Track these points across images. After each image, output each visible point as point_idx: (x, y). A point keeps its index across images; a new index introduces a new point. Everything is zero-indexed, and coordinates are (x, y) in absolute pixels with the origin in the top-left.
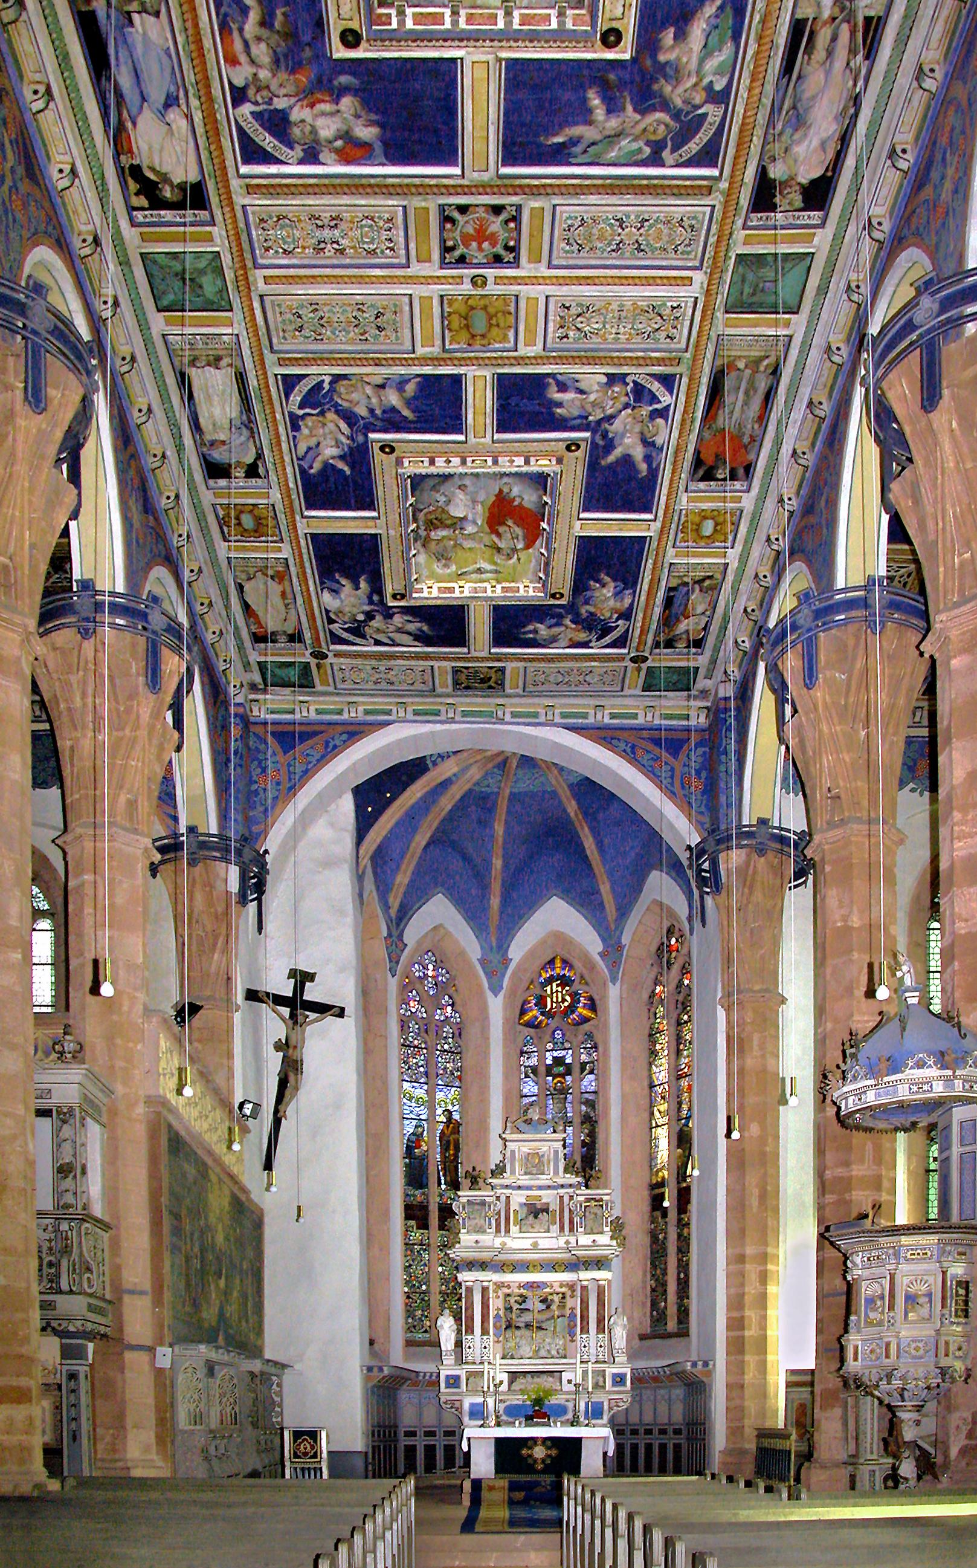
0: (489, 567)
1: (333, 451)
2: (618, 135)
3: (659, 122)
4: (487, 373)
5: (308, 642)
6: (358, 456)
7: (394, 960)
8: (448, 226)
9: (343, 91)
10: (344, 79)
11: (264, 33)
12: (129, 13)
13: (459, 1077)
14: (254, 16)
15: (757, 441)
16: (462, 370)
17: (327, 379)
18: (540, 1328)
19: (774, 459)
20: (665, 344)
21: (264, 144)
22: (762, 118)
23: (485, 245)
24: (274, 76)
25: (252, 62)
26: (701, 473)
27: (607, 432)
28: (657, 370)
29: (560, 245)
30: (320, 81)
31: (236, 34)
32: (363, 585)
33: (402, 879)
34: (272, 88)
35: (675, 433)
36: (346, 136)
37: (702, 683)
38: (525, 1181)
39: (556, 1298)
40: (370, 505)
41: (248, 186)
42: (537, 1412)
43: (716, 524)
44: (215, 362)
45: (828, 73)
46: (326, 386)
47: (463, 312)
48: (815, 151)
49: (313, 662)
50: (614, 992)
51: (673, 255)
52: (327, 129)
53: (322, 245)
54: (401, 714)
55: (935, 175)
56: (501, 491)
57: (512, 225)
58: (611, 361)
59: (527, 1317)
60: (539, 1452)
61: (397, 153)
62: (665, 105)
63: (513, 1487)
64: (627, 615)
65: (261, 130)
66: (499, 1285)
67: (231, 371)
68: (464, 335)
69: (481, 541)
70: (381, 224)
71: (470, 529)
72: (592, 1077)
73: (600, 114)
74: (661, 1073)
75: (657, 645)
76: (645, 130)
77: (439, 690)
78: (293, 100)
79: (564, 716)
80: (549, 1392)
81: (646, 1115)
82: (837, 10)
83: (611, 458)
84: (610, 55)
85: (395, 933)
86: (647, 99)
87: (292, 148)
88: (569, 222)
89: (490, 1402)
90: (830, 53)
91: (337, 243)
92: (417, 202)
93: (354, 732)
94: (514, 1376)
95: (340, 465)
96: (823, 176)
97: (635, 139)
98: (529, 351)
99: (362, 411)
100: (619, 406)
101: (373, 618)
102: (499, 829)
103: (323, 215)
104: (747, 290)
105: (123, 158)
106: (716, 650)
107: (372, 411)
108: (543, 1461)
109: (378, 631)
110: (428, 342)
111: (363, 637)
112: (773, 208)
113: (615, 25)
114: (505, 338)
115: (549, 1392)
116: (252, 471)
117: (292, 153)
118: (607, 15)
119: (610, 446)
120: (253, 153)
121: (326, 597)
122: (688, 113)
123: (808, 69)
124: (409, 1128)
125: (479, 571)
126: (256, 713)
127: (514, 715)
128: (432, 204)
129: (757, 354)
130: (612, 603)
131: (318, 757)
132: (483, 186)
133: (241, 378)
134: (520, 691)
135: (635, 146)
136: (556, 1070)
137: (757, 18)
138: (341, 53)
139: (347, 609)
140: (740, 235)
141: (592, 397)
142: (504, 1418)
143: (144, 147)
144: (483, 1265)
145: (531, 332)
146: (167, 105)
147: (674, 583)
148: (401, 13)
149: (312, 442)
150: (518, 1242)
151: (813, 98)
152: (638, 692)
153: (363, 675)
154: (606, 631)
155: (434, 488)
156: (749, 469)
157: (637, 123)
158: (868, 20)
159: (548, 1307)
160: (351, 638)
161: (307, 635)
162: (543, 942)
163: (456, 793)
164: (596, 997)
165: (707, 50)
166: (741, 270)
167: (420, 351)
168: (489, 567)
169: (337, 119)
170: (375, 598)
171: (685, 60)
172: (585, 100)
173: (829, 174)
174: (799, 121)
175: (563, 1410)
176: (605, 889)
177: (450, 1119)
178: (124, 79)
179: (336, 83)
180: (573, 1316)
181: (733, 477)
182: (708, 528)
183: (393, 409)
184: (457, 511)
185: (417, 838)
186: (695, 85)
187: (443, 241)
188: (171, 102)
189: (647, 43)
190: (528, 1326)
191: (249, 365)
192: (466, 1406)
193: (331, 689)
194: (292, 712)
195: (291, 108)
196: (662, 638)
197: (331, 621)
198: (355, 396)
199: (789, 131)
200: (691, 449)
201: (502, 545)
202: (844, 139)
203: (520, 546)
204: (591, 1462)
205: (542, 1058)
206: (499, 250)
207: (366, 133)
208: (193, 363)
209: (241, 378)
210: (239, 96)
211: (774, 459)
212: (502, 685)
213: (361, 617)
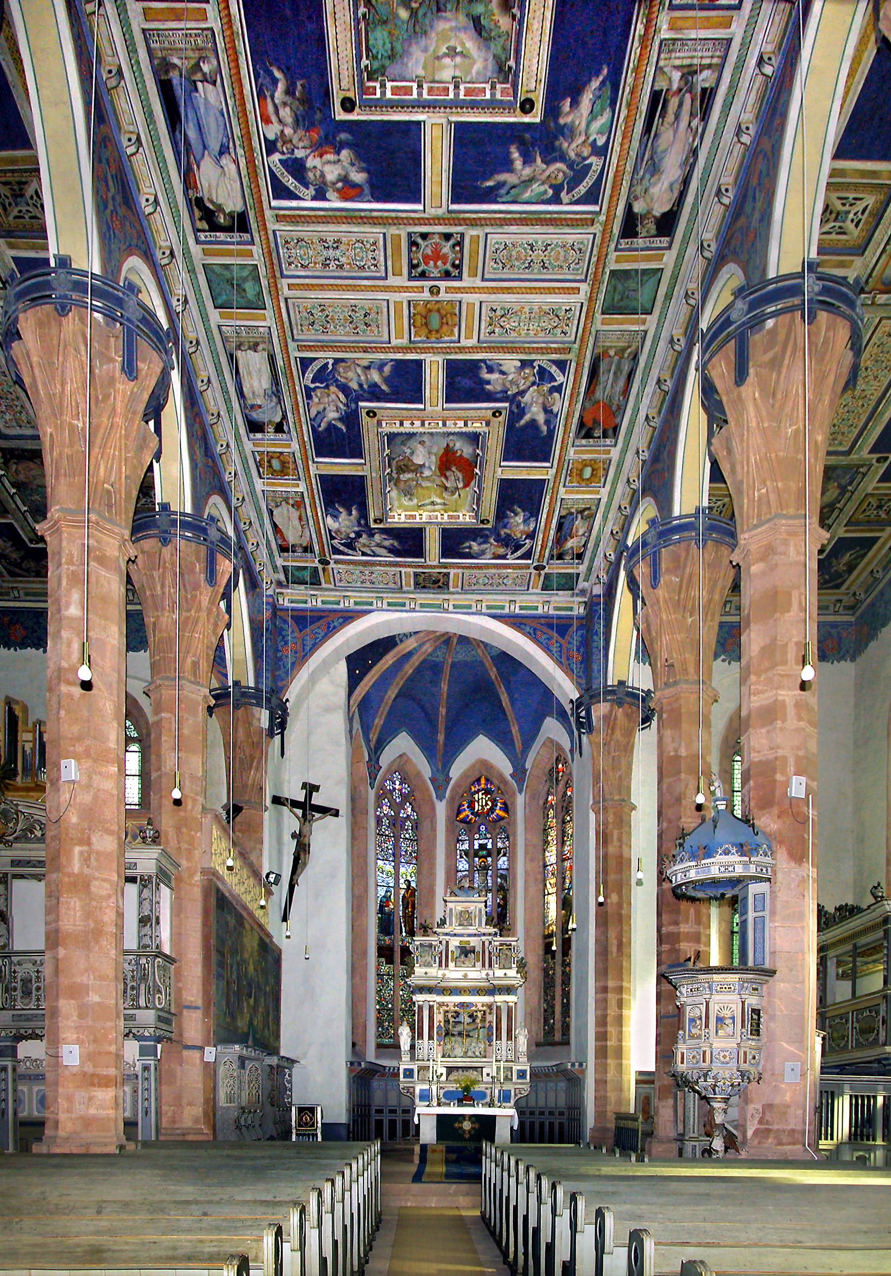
0: (439, 501)
1: (336, 415)
2: (531, 180)
3: (559, 170)
4: (440, 358)
5: (317, 552)
6: (351, 418)
7: (373, 776)
10: (343, 136)
11: (289, 99)
13: (416, 858)
14: (281, 86)
15: (622, 409)
16: (422, 356)
17: (331, 362)
18: (468, 1036)
19: (632, 423)
20: (560, 337)
21: (288, 184)
22: (629, 168)
23: (439, 263)
25: (280, 121)
26: (583, 432)
27: (520, 402)
28: (554, 357)
29: (490, 264)
30: (326, 136)
32: (354, 512)
33: (379, 722)
34: (294, 142)
35: (566, 404)
36: (345, 179)
37: (582, 584)
38: (459, 930)
39: (479, 1014)
40: (360, 456)
42: (466, 1096)
43: (593, 470)
44: (254, 347)
45: (675, 132)
46: (330, 367)
47: (424, 313)
48: (666, 191)
49: (320, 567)
50: (520, 800)
52: (332, 174)
54: (380, 604)
55: (748, 208)
57: (458, 248)
58: (523, 350)
59: (459, 1028)
60: (467, 1125)
62: (563, 158)
63: (449, 1150)
64: (532, 536)
66: (441, 1005)
67: (265, 354)
68: (424, 331)
69: (434, 481)
70: (368, 246)
71: (427, 473)
72: (505, 858)
73: (518, 164)
74: (551, 857)
75: (552, 557)
77: (405, 589)
78: (308, 151)
79: (488, 607)
80: (475, 1082)
81: (541, 886)
82: (683, 83)
83: (522, 422)
84: (527, 119)
85: (374, 759)
86: (552, 153)
89: (434, 1088)
90: (677, 117)
92: (393, 230)
93: (348, 617)
94: (450, 1070)
95: (340, 425)
97: (543, 183)
98: (468, 342)
99: (354, 386)
100: (528, 384)
101: (361, 536)
102: (444, 687)
104: (617, 297)
106: (592, 561)
107: (361, 385)
108: (469, 1131)
109: (364, 545)
110: (399, 336)
111: (354, 549)
112: (635, 235)
113: (530, 96)
114: (452, 333)
115: (475, 1082)
116: (279, 428)
118: (525, 89)
119: (522, 412)
120: (281, 191)
121: (329, 520)
124: (382, 892)
125: (433, 503)
126: (281, 602)
127: (455, 607)
128: (402, 232)
129: (621, 344)
130: (522, 527)
131: (322, 634)
132: (439, 219)
133: (272, 359)
134: (459, 590)
135: (542, 188)
136: (481, 853)
137: (627, 90)
138: (341, 115)
139: (343, 529)
140: (613, 255)
141: (510, 377)
142: (443, 1100)
143: (205, 184)
144: (430, 990)
145: (470, 328)
146: (221, 153)
147: (564, 513)
148: (383, 86)
149: (321, 408)
150: (454, 974)
152: (539, 591)
153: (354, 577)
154: (518, 547)
155: (403, 443)
156: (616, 430)
157: (544, 171)
158: (704, 90)
159: (474, 1021)
160: (346, 550)
161: (316, 548)
162: (472, 767)
163: (416, 660)
164: (508, 803)
165: (593, 115)
166: (613, 281)
167: (395, 342)
168: (439, 501)
170: (362, 522)
171: (577, 123)
172: (509, 153)
174: (655, 169)
175: (483, 1095)
176: (515, 730)
177: (409, 886)
180: (491, 1027)
181: (605, 436)
182: (588, 472)
183: (375, 385)
184: (418, 460)
185: (389, 693)
187: (410, 260)
188: (224, 150)
189: (552, 111)
190: (460, 1034)
191: (277, 350)
192: (417, 1092)
193: (332, 586)
194: (306, 602)
195: (307, 157)
196: (555, 552)
197: (332, 538)
198: (350, 374)
199: (648, 176)
200: (577, 415)
201: (448, 485)
203: (460, 485)
204: (503, 1133)
205: (471, 845)
206: (448, 267)
207: (358, 177)
208: (239, 347)
209: (272, 359)
210: (271, 147)
211: (632, 423)
212: (448, 585)
213: (353, 535)
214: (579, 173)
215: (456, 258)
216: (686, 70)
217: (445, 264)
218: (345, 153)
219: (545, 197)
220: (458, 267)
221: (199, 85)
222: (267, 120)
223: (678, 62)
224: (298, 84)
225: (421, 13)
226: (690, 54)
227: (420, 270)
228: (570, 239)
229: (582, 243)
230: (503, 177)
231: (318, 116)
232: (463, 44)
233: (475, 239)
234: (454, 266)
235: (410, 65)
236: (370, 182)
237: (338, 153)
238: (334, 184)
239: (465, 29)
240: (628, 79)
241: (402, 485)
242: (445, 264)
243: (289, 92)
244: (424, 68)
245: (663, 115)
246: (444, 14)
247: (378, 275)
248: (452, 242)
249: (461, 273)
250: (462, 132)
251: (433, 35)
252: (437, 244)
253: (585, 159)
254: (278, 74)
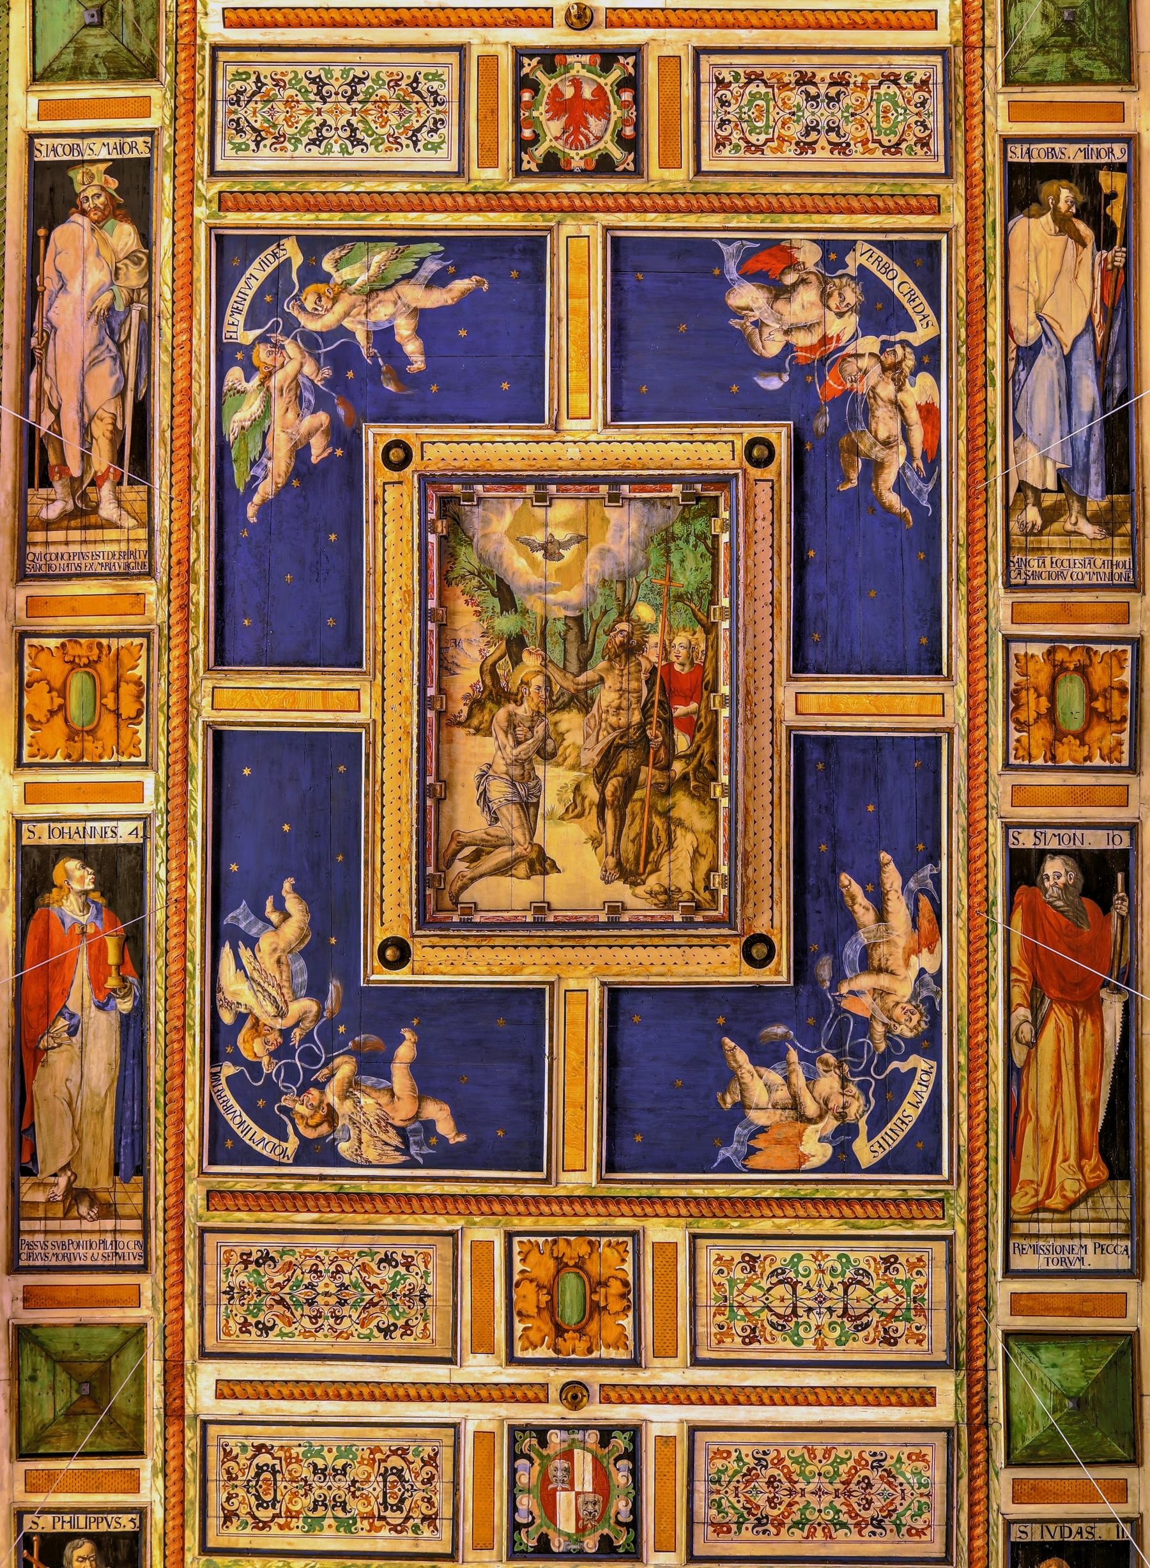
2: (371, 292)
3: (315, 315)
8: (629, 131)
9: (774, 366)
10: (773, 383)
11: (878, 453)
12: (1060, 489)
14: (889, 477)
21: (902, 276)
22: (164, 330)
23: (569, 92)
24: (873, 388)
29: (448, 90)
31: (918, 452)
36: (780, 292)
41: (937, 211)
45: (83, 403)
48: (73, 277)
51: (265, 71)
53: (833, 91)
57: (527, 133)
61: (704, 252)
62: (310, 342)
65: (904, 301)
70: (736, 136)
73: (404, 328)
76: (335, 300)
78: (850, 350)
82: (93, 497)
84: (395, 431)
86: (335, 350)
87: (861, 268)
88: (436, 138)
90: (86, 431)
91: (809, 97)
96: (50, 229)
97: (346, 284)
103: (826, 154)
105: (1120, 262)
112: (116, 168)
117: (863, 260)
118: (405, 488)
120: (920, 259)
122: (272, 330)
123: (111, 408)
132: (574, 210)
135: (346, 273)
151: (95, 362)
157: (347, 314)
165: (261, 426)
166: (146, 47)
169: (789, 319)
171: (291, 415)
172: (427, 352)
173: (42, 232)
174: (109, 322)
178: (1088, 390)
179: (786, 378)
186: (269, 375)
187: (637, 101)
189: (346, 440)
195: (854, 337)
199: (120, 307)
202: (33, 296)
206: (547, 83)
207: (747, 296)
210: (928, 357)
214: (269, 309)
215: (531, 106)
216: (93, 519)
217: (556, 90)
218: (772, 347)
219: (336, 253)
220: (523, 83)
221: (1051, 484)
222: (929, 412)
223: (112, 534)
224: (855, 482)
225: (613, 615)
226: (91, 548)
227: (616, 74)
228: (265, 159)
229: (238, 148)
230: (437, 298)
231: (822, 422)
232: (533, 563)
233: (489, 158)
234: (535, 87)
235: (634, 525)
236: (726, 286)
237: (788, 348)
238: (803, 281)
239: (529, 590)
240: (203, 505)
242: (556, 90)
243: (873, 468)
244: (605, 520)
245: (117, 435)
246: (570, 614)
247: (716, 59)
248: (540, 151)
249: (518, 66)
250: (527, 406)
251: (591, 579)
252: (577, 145)
253: (263, 339)
254: (893, 499)
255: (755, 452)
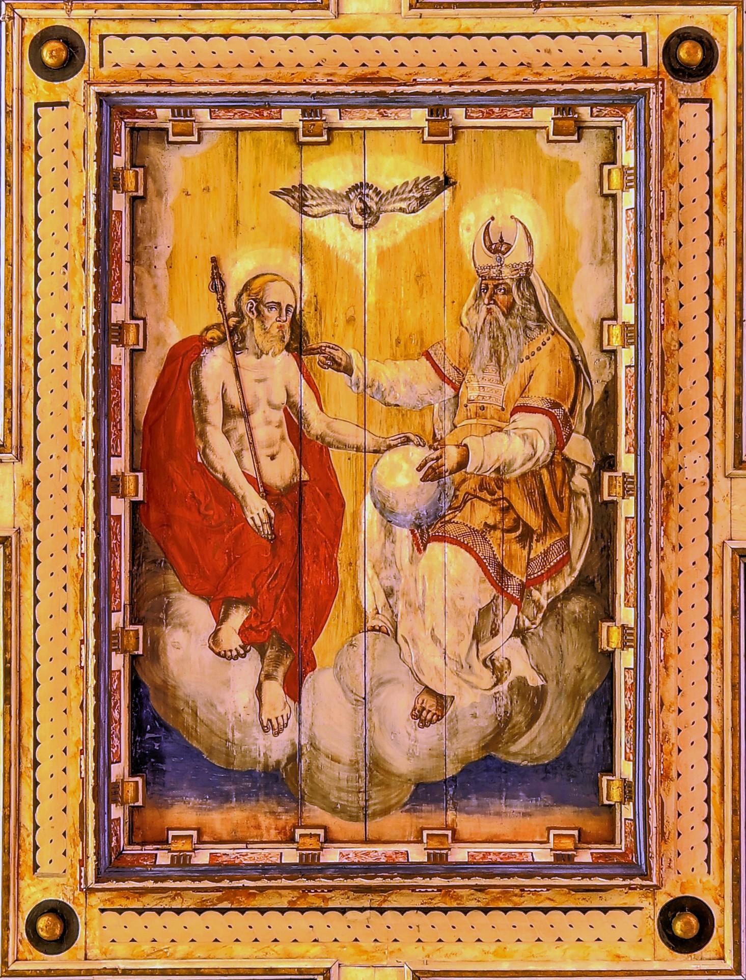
56: (294, 688)
71: (400, 474)
155: (532, 699)
203: (215, 364)
241: (544, 373)
255: (678, 927)
